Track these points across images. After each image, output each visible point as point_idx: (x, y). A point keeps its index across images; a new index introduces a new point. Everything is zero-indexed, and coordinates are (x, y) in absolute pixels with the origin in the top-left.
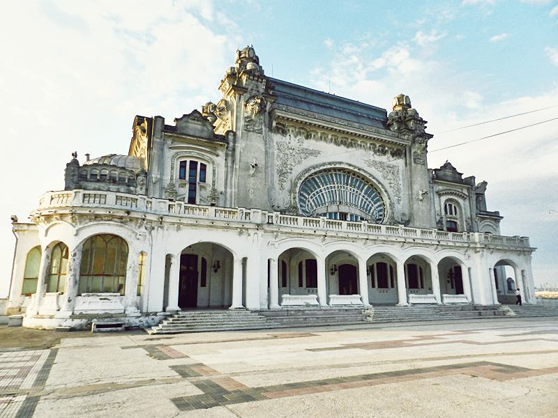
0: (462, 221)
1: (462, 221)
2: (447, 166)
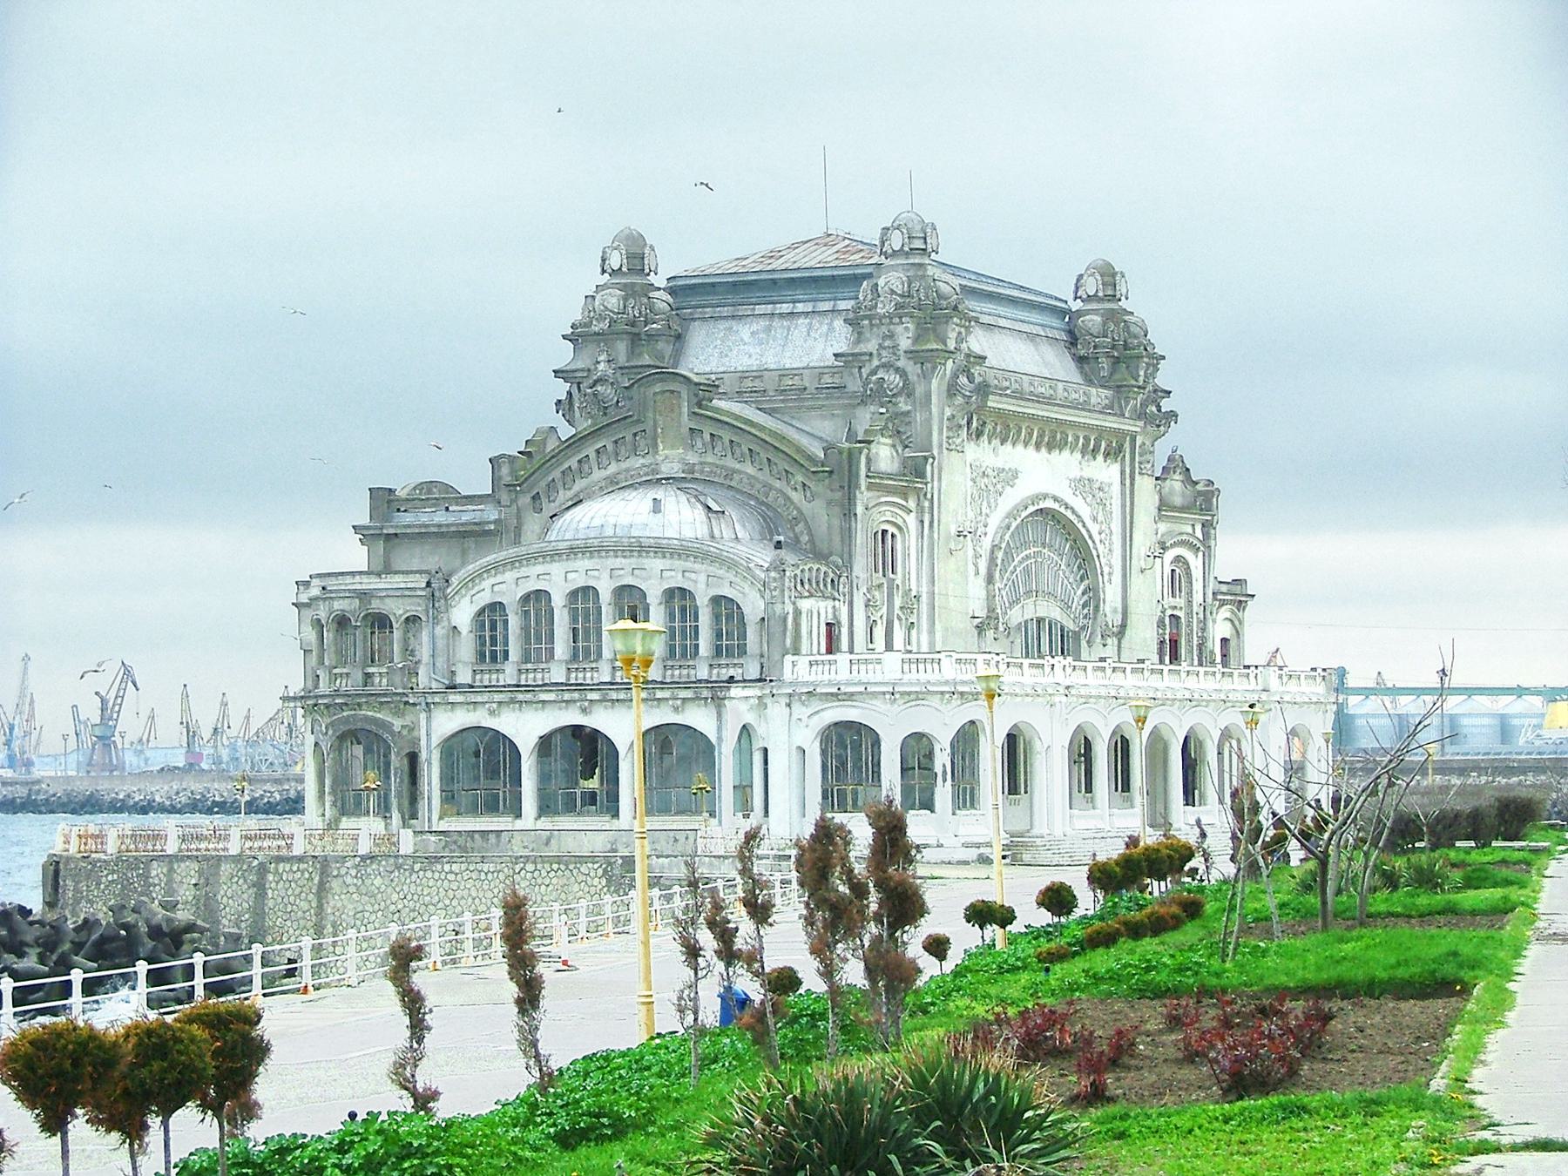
0: (1190, 614)
1: (1190, 614)
2: (1175, 465)
